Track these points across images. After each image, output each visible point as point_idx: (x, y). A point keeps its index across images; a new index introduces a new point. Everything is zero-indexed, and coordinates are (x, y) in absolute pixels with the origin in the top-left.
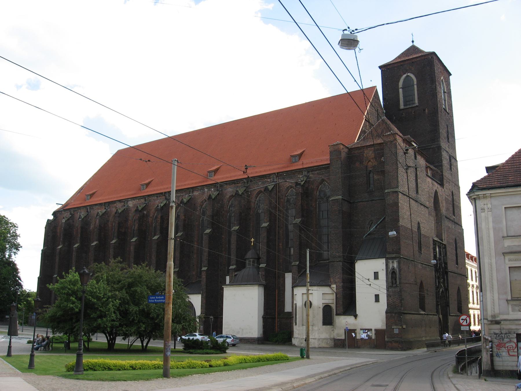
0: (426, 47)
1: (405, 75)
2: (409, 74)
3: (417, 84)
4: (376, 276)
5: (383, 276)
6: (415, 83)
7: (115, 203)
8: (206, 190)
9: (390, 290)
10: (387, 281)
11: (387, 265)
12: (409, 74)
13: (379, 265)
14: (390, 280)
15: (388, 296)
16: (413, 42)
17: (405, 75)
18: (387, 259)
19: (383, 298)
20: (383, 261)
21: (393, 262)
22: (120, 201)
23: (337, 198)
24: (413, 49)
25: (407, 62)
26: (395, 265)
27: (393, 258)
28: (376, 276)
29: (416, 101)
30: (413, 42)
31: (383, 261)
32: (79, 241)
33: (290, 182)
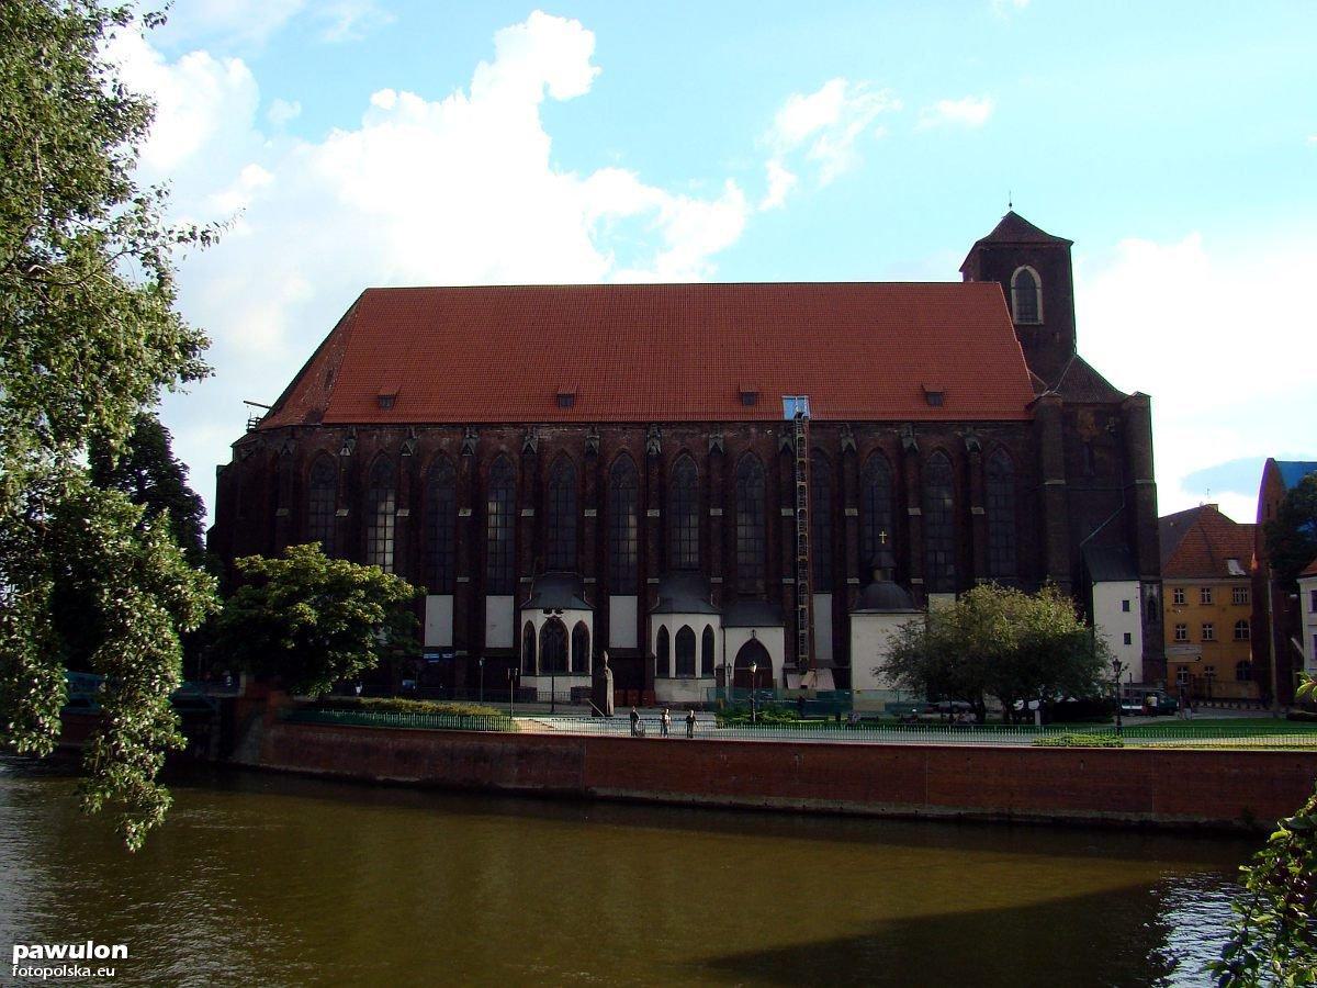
0: (1050, 223)
1: (1020, 269)
2: (1027, 268)
3: (1043, 288)
4: (1126, 606)
5: (1136, 606)
6: (1039, 285)
7: (497, 428)
8: (753, 430)
9: (1148, 627)
10: (1143, 615)
11: (1142, 591)
12: (1027, 268)
13: (1130, 590)
14: (1147, 613)
15: (1145, 636)
16: (1011, 205)
17: (1020, 269)
18: (1142, 582)
19: (1137, 639)
20: (1137, 584)
21: (1151, 587)
22: (515, 425)
23: (1057, 482)
24: (1013, 223)
25: (1026, 246)
26: (1155, 592)
27: (1152, 582)
28: (1126, 606)
29: (1040, 316)
30: (1011, 205)
31: (1137, 584)
32: (405, 503)
33: (934, 441)
